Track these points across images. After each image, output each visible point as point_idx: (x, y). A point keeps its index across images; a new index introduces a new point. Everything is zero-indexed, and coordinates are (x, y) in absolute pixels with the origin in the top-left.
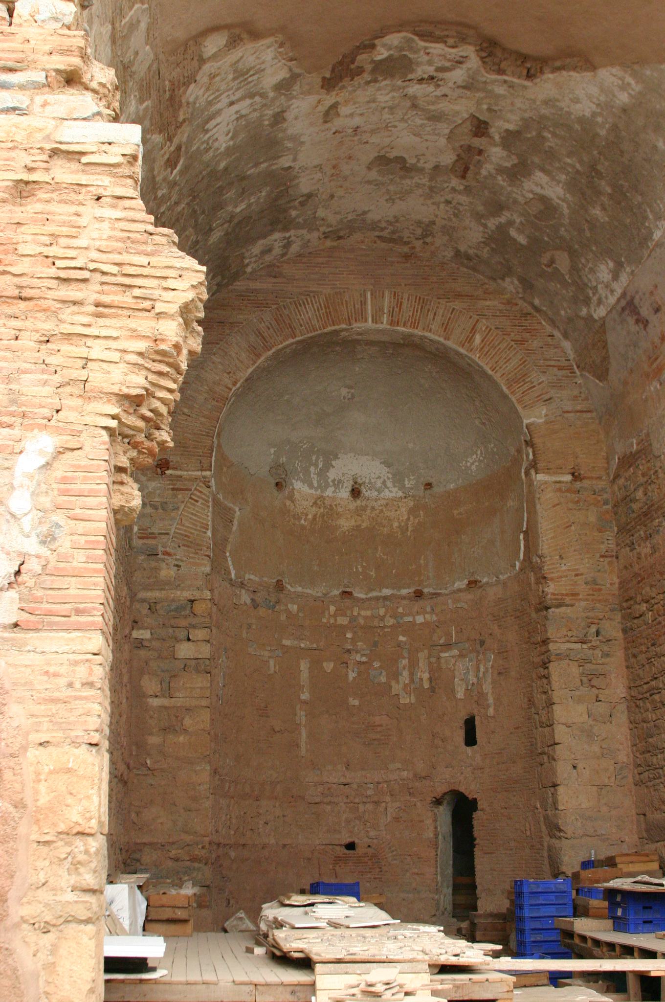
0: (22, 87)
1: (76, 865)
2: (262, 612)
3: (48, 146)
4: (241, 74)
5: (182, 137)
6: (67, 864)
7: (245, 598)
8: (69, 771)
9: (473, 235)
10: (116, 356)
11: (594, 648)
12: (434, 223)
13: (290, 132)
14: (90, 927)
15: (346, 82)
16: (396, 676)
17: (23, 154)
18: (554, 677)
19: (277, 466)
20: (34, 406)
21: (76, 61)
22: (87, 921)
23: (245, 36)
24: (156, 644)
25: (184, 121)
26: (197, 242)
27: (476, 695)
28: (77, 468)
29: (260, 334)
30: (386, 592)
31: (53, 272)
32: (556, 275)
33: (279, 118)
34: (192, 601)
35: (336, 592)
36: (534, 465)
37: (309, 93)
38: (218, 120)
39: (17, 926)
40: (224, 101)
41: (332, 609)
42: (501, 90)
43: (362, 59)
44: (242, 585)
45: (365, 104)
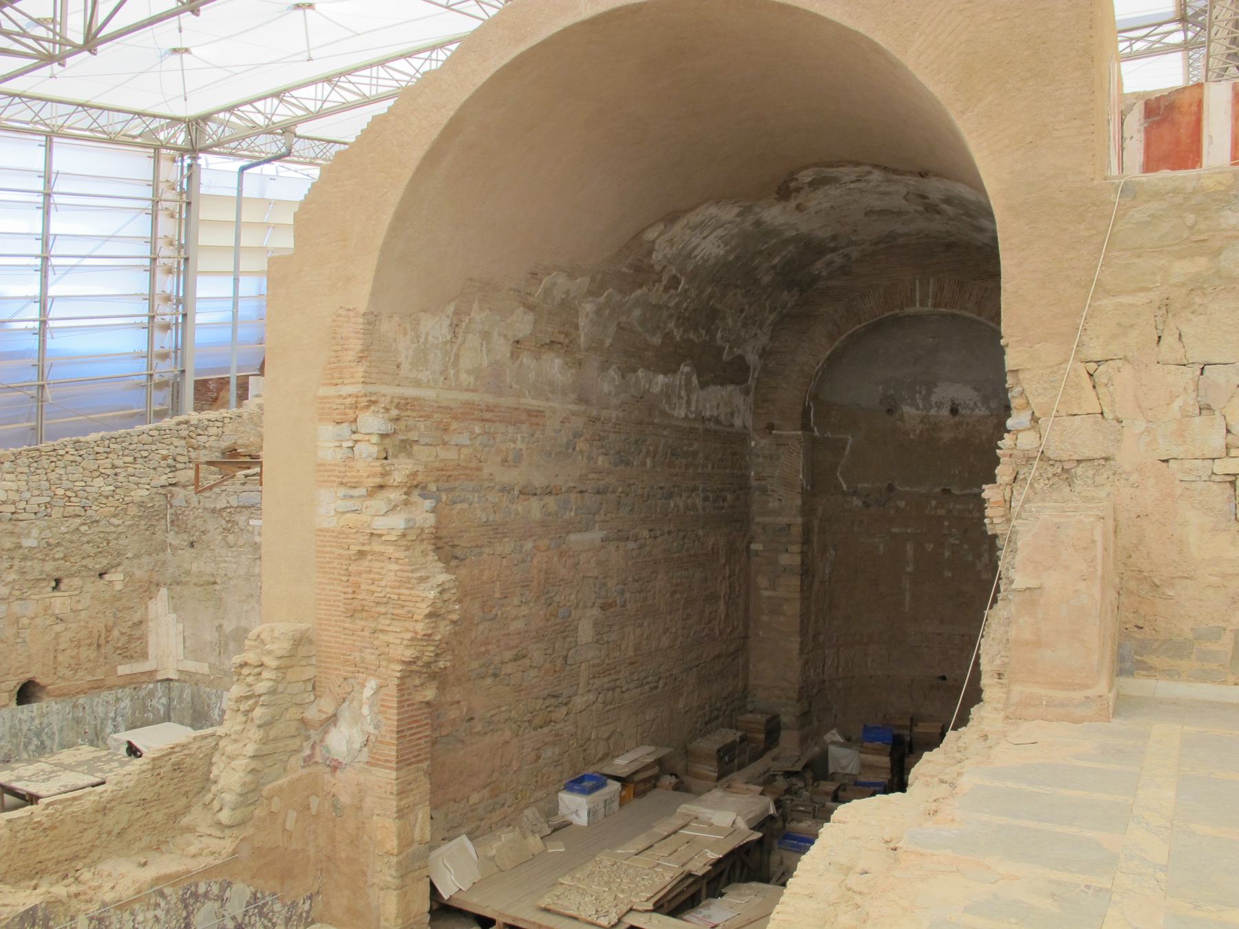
3: (369, 531)
7: (857, 502)
10: (399, 641)
16: (979, 556)
35: (937, 490)
41: (934, 503)
44: (855, 493)
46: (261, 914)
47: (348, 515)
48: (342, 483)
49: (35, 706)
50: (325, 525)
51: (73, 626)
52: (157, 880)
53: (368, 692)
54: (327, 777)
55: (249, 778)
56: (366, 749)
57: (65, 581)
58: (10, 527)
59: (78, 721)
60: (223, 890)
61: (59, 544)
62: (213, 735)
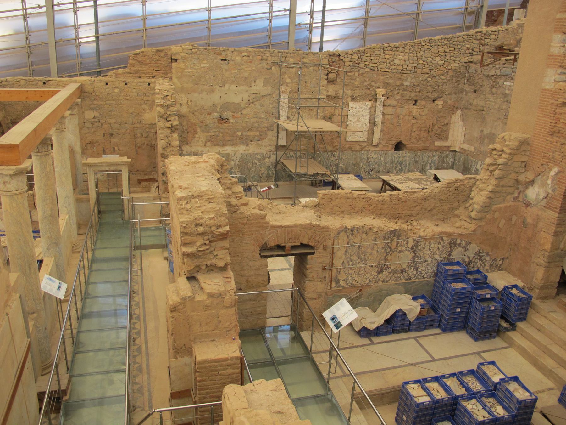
46: (480, 259)
47: (561, 83)
48: (561, 66)
49: (401, 152)
50: (547, 87)
51: (419, 121)
52: (441, 233)
53: (552, 173)
54: (523, 208)
55: (487, 201)
56: (545, 200)
57: (419, 102)
58: (399, 76)
59: (416, 162)
60: (467, 244)
61: (418, 85)
62: (474, 178)
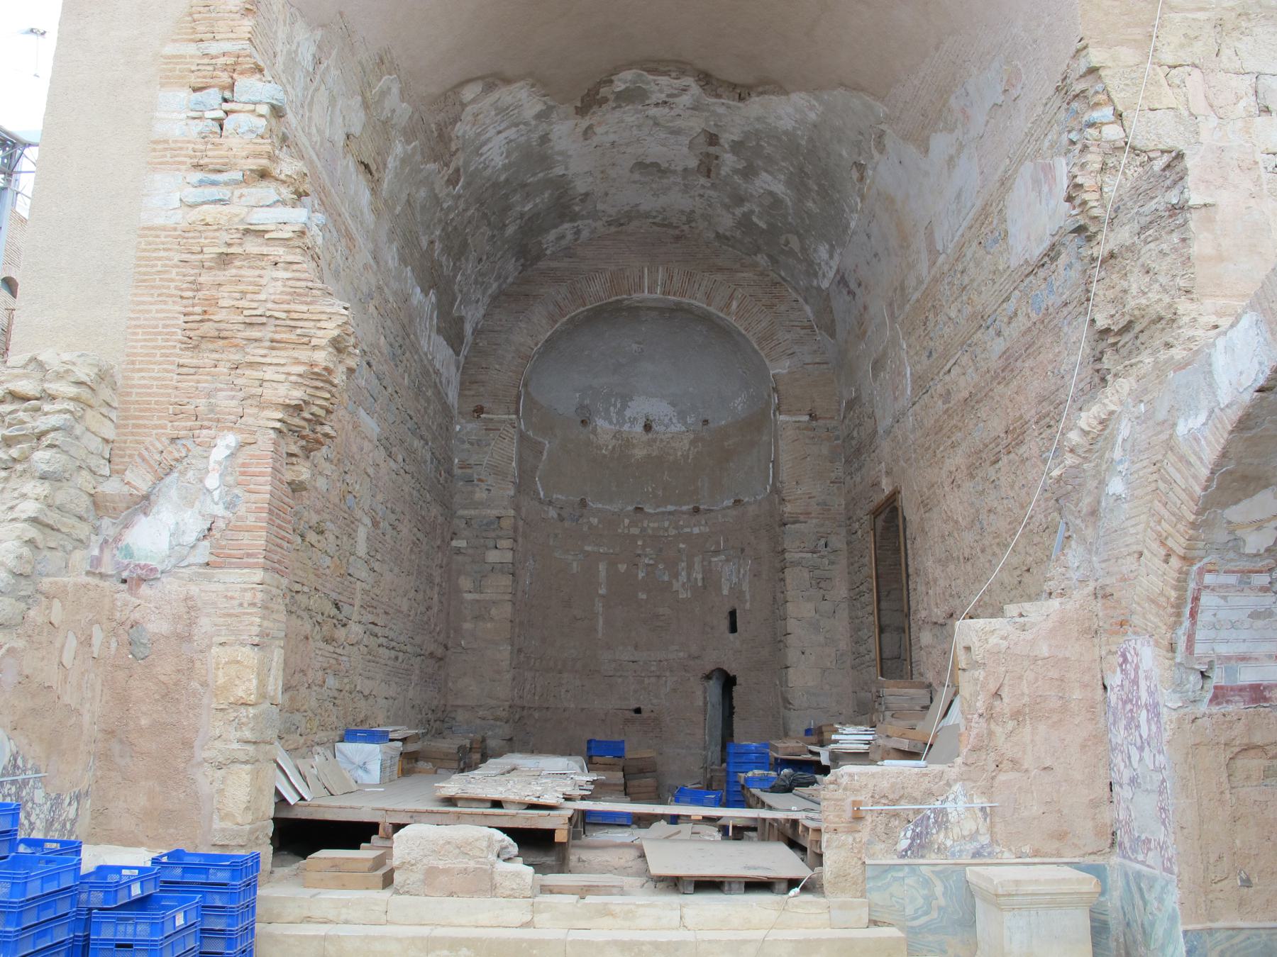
0: (226, 184)
1: (241, 725)
2: (567, 524)
3: (241, 227)
4: (502, 111)
5: (458, 161)
6: (234, 724)
7: (553, 513)
8: (238, 662)
9: (726, 222)
10: (282, 377)
11: (823, 557)
12: (694, 211)
13: (557, 149)
14: (248, 767)
15: (595, 108)
16: (676, 575)
17: (224, 233)
18: (788, 581)
19: (582, 407)
20: (224, 413)
21: (264, 162)
22: (246, 762)
23: (497, 82)
24: (470, 551)
25: (457, 150)
26: (494, 236)
27: (737, 592)
28: (252, 457)
29: (557, 304)
30: (670, 508)
31: (241, 319)
32: (791, 253)
33: (545, 139)
34: (499, 518)
35: (630, 508)
36: (778, 408)
37: (566, 118)
38: (490, 145)
39: (200, 764)
40: (492, 132)
41: (627, 521)
42: (721, 110)
43: (604, 91)
44: (550, 503)
45: (614, 124)
47: (205, 207)
50: (159, 221)
53: (219, 453)
